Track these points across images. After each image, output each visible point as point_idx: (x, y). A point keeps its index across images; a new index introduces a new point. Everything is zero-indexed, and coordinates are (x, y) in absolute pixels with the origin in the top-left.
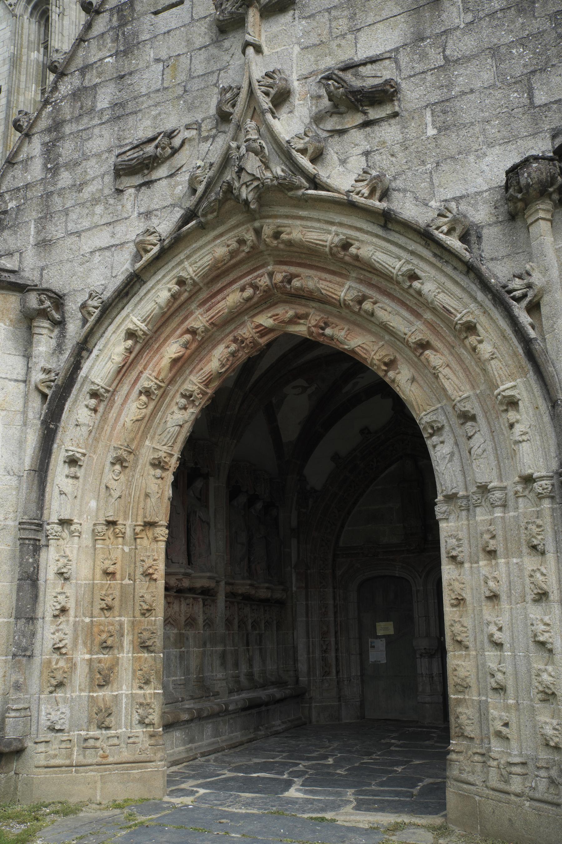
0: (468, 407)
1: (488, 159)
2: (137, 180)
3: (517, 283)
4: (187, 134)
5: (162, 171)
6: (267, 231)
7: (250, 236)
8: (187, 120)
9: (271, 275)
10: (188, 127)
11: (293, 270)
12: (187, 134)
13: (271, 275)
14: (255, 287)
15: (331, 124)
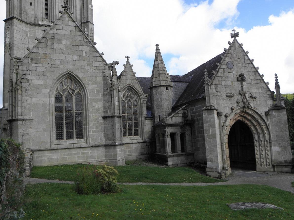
0: (260, 132)
1: (263, 108)
2: (230, 98)
3: (267, 123)
4: (236, 94)
5: (232, 98)
6: (245, 110)
7: (243, 110)
8: (235, 92)
9: (242, 114)
10: (235, 93)
11: (244, 114)
12: (236, 94)
13: (242, 114)
14: (240, 115)
15: (251, 99)
